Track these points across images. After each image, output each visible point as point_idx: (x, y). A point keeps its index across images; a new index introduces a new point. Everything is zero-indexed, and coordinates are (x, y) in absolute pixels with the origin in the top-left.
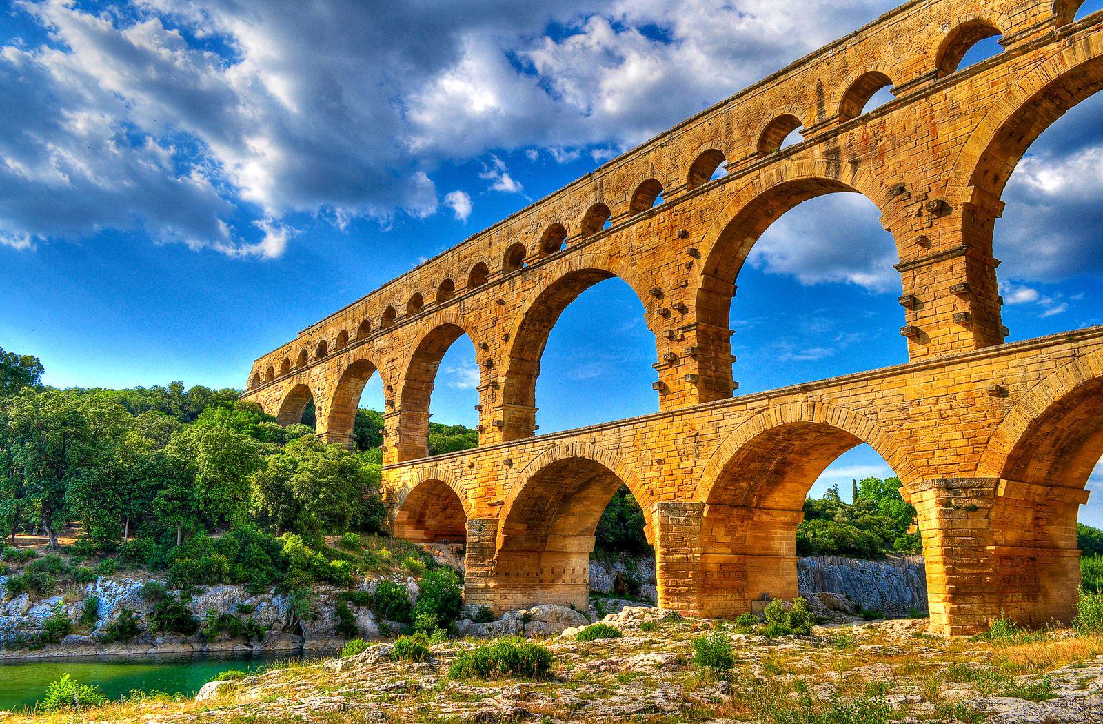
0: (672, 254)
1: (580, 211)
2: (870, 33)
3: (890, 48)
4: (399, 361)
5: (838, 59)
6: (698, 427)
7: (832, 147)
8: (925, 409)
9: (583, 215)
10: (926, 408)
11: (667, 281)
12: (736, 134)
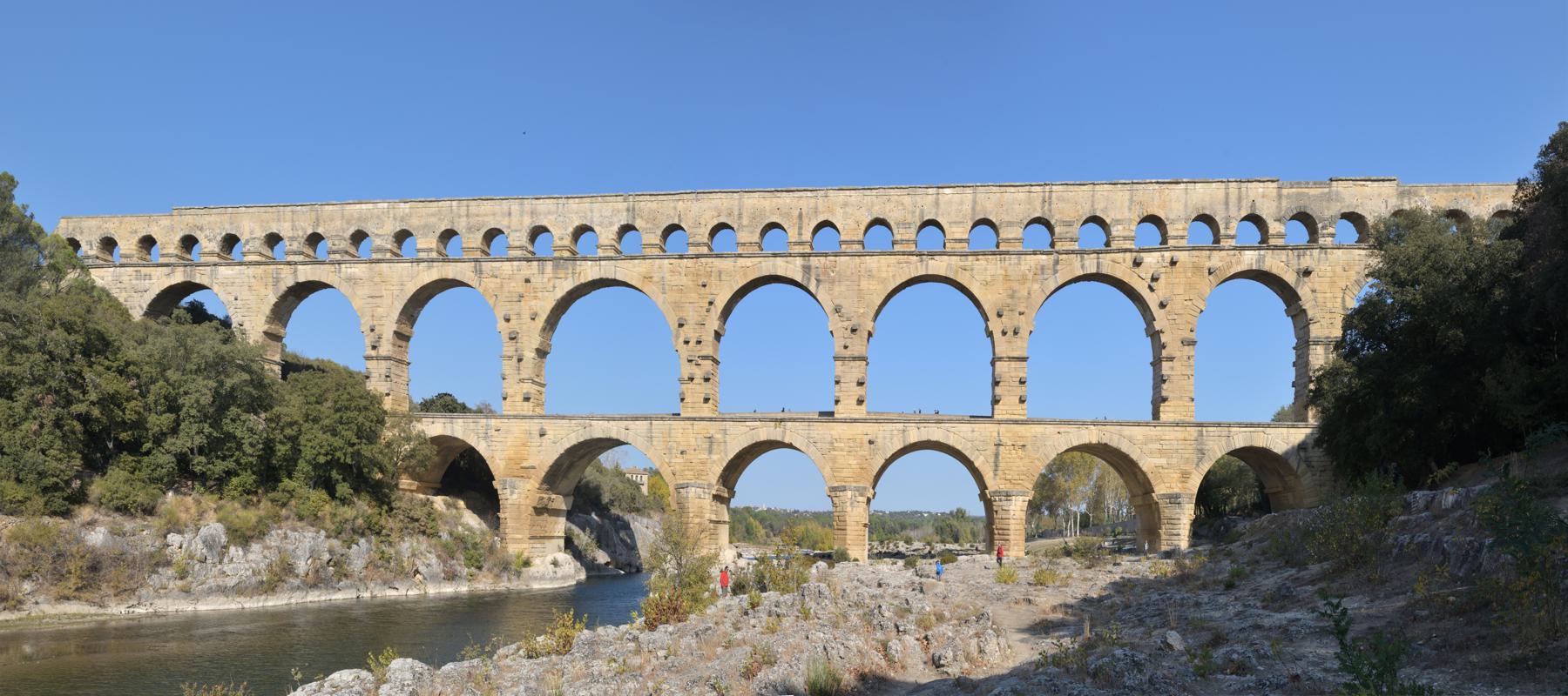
0: (694, 295)
1: (611, 224)
4: (387, 301)
11: (692, 316)
12: (745, 222)
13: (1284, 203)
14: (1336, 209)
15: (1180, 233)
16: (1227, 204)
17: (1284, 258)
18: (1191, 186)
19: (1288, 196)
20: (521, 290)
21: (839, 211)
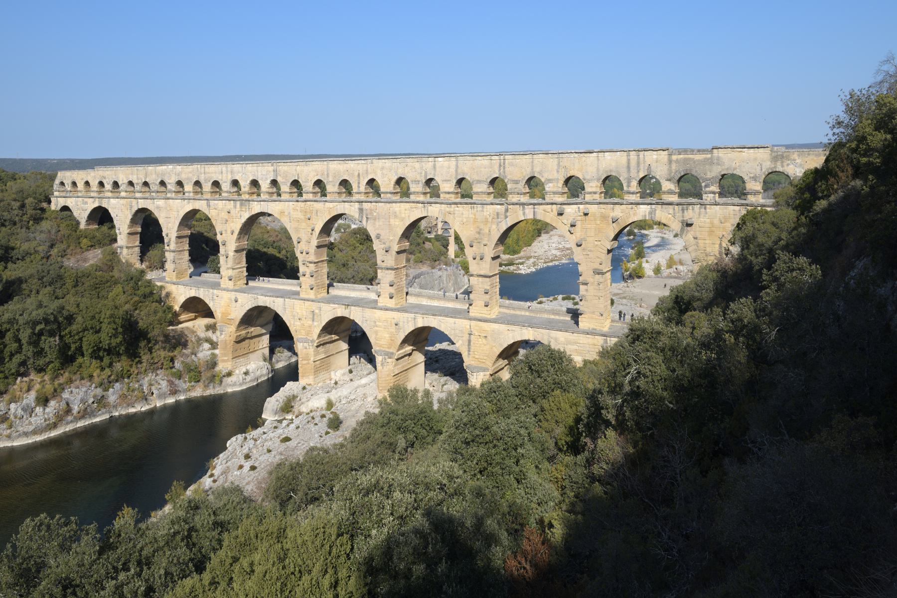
1: (266, 179)
9: (269, 181)
13: (674, 166)
14: (715, 172)
15: (594, 190)
16: (629, 167)
17: (671, 211)
18: (601, 154)
19: (677, 161)
20: (226, 217)
21: (379, 172)
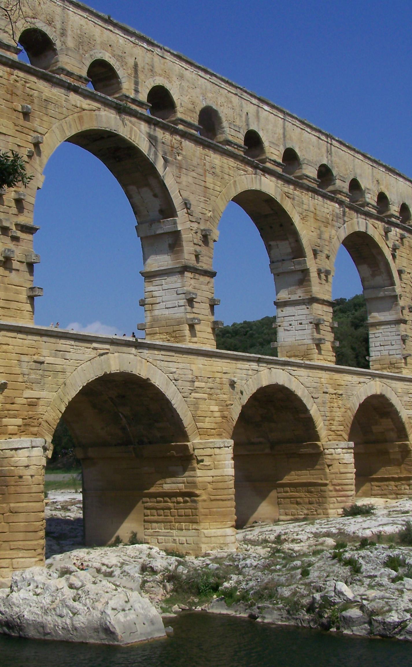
0: (12, 126)
2: (168, 56)
3: (178, 83)
5: (149, 54)
6: (45, 352)
7: (152, 133)
8: (203, 385)
10: (203, 385)
